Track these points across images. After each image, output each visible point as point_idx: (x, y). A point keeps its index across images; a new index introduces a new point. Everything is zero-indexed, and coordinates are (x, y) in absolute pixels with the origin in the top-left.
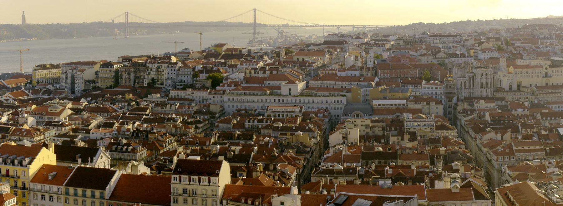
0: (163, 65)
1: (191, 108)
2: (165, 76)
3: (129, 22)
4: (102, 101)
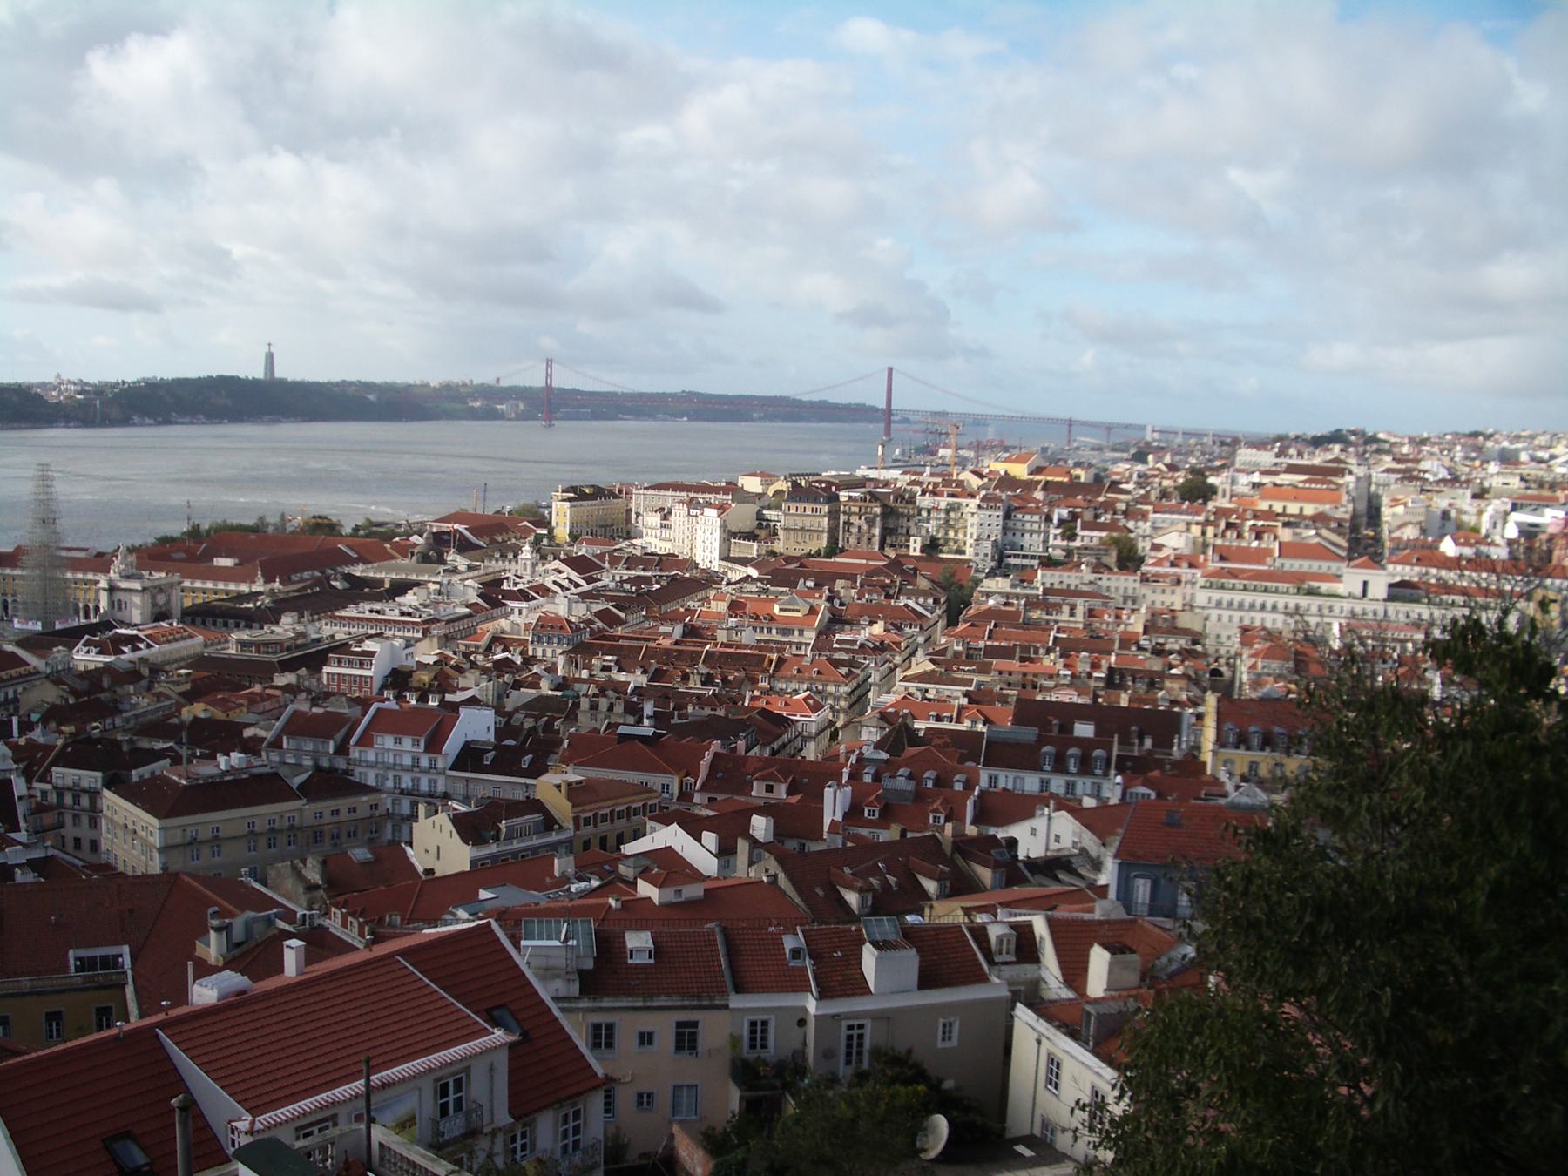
2: (969, 530)
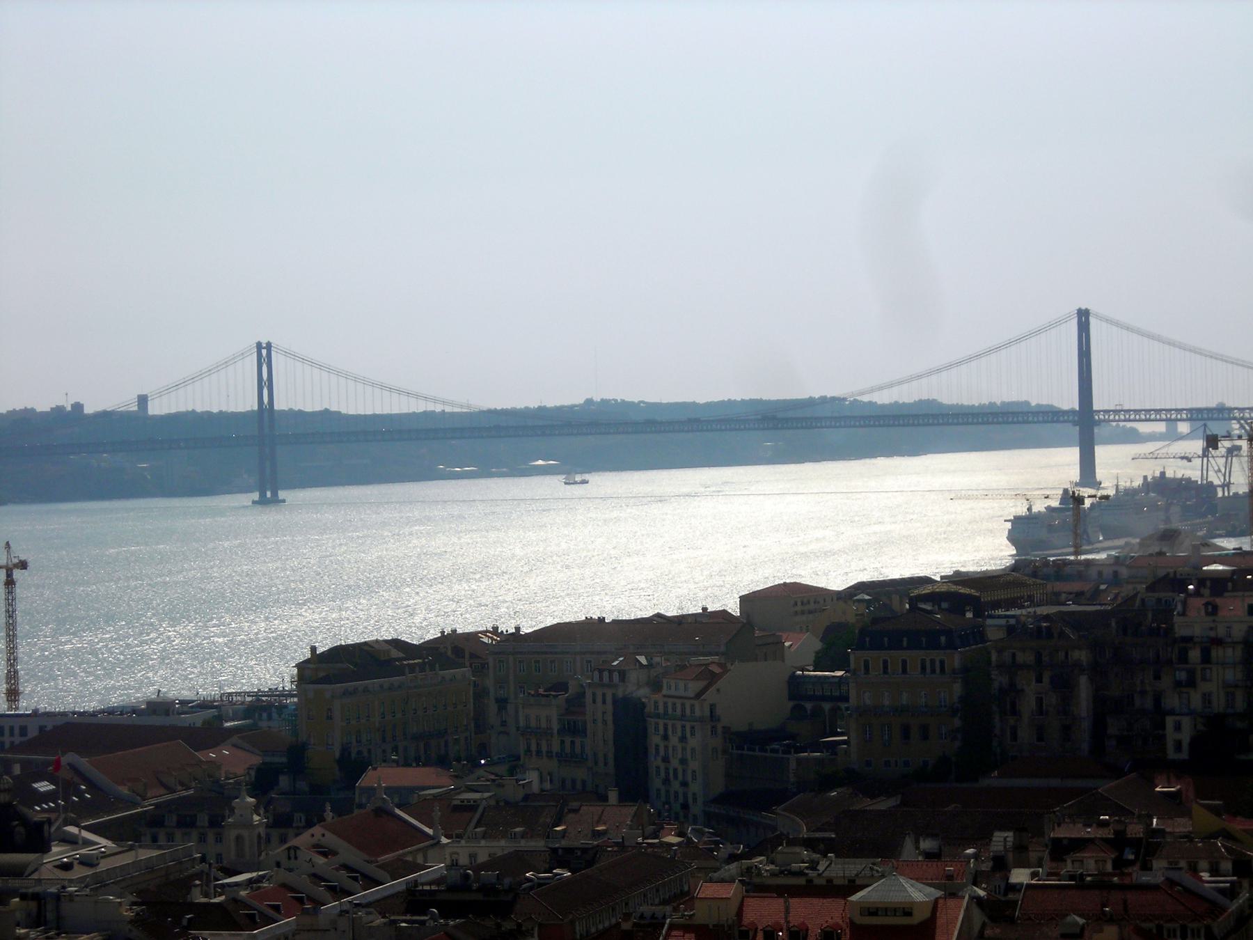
3: (280, 405)
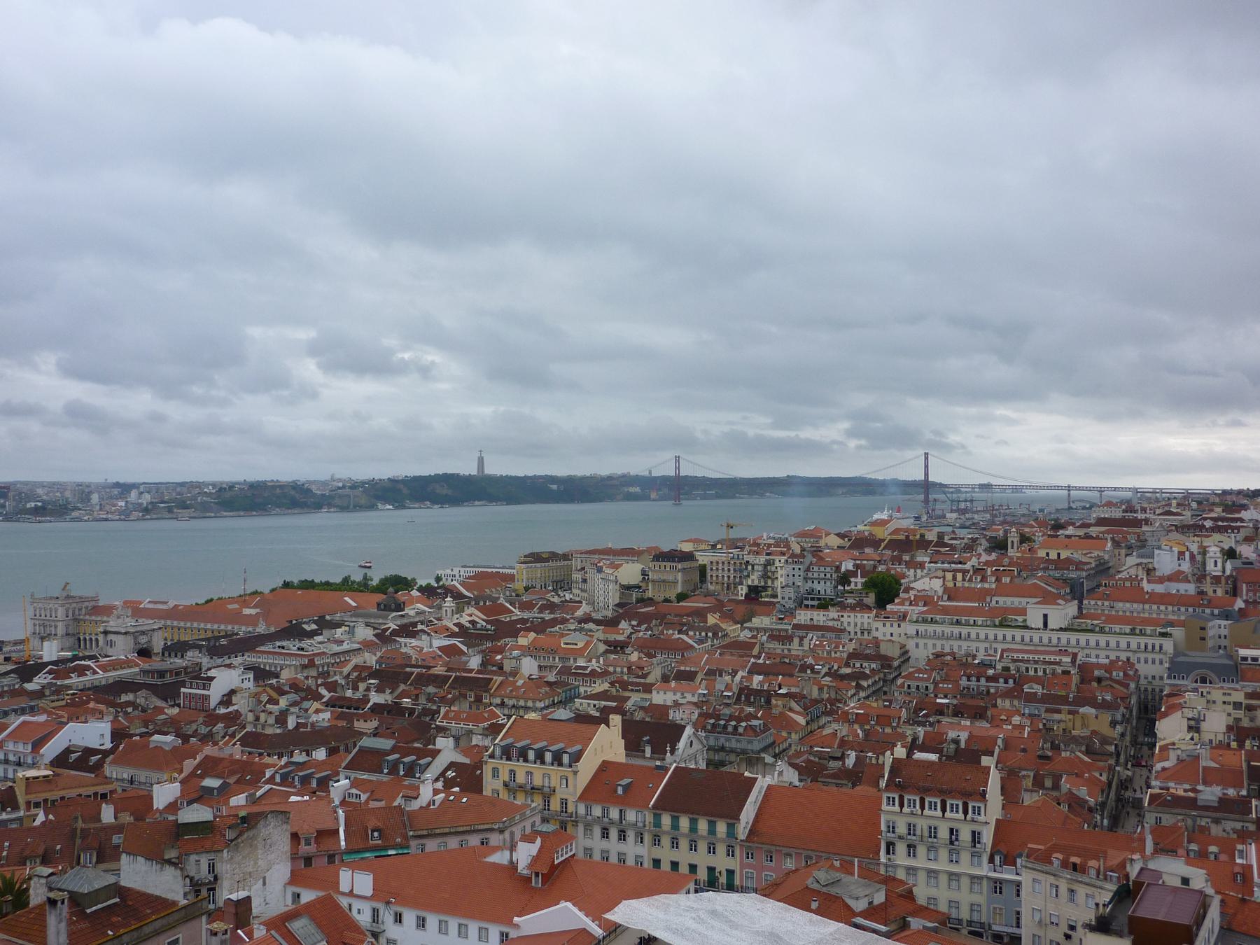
0: (777, 558)
1: (841, 646)
2: (780, 579)
4: (660, 628)
